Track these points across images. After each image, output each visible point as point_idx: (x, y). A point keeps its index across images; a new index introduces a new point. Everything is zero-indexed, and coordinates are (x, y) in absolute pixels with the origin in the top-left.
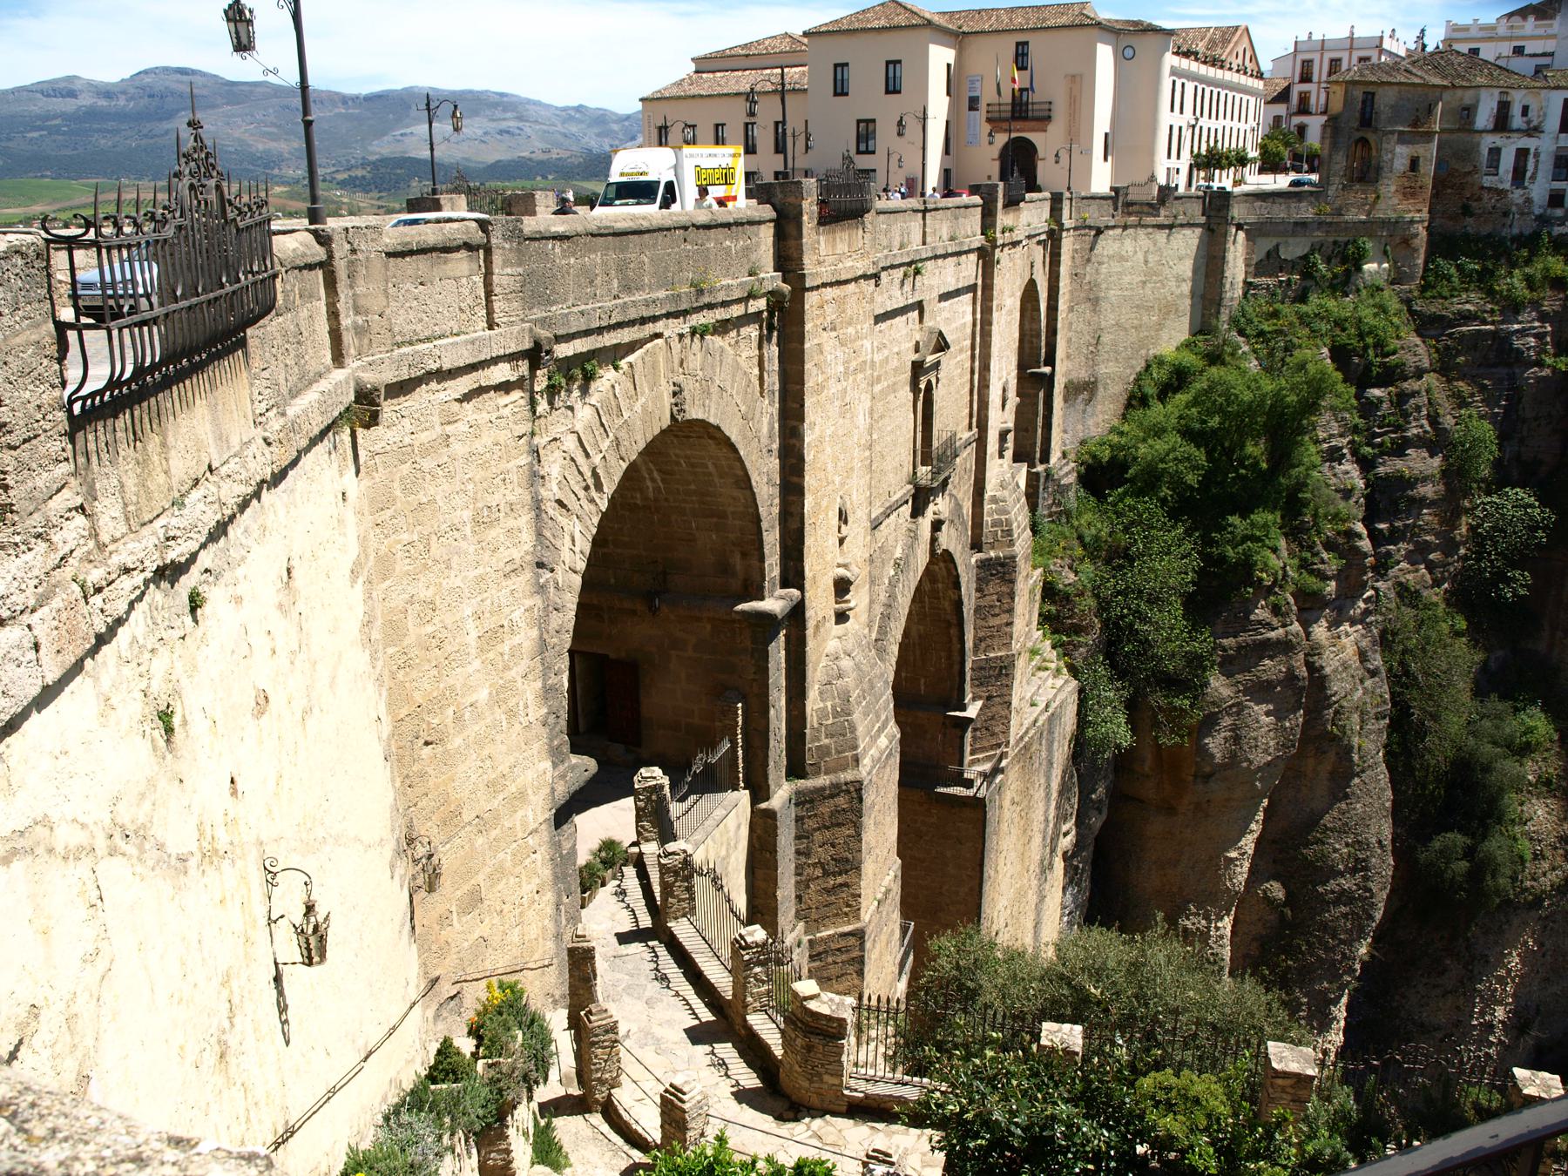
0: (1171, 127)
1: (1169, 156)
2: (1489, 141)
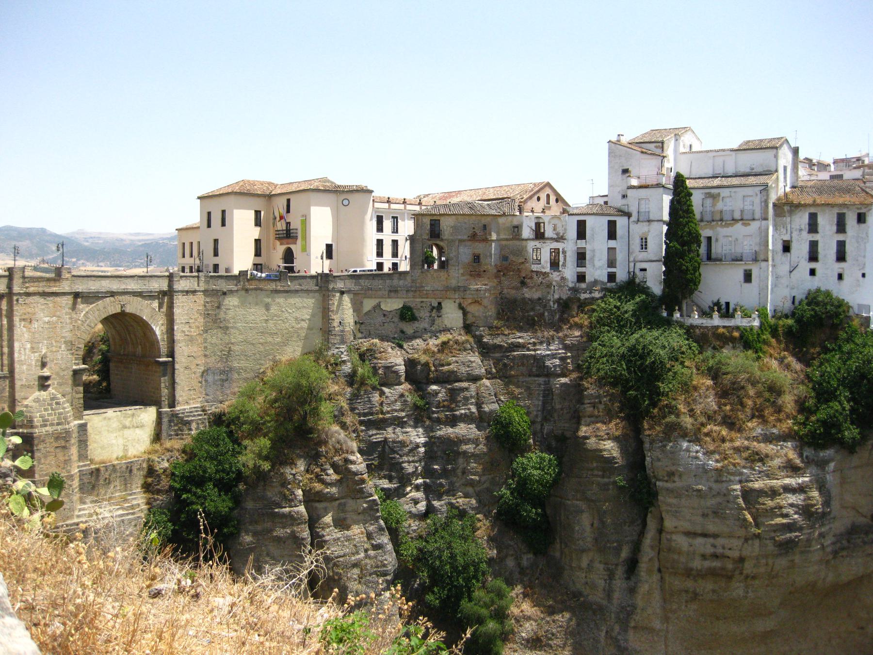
2: (531, 245)
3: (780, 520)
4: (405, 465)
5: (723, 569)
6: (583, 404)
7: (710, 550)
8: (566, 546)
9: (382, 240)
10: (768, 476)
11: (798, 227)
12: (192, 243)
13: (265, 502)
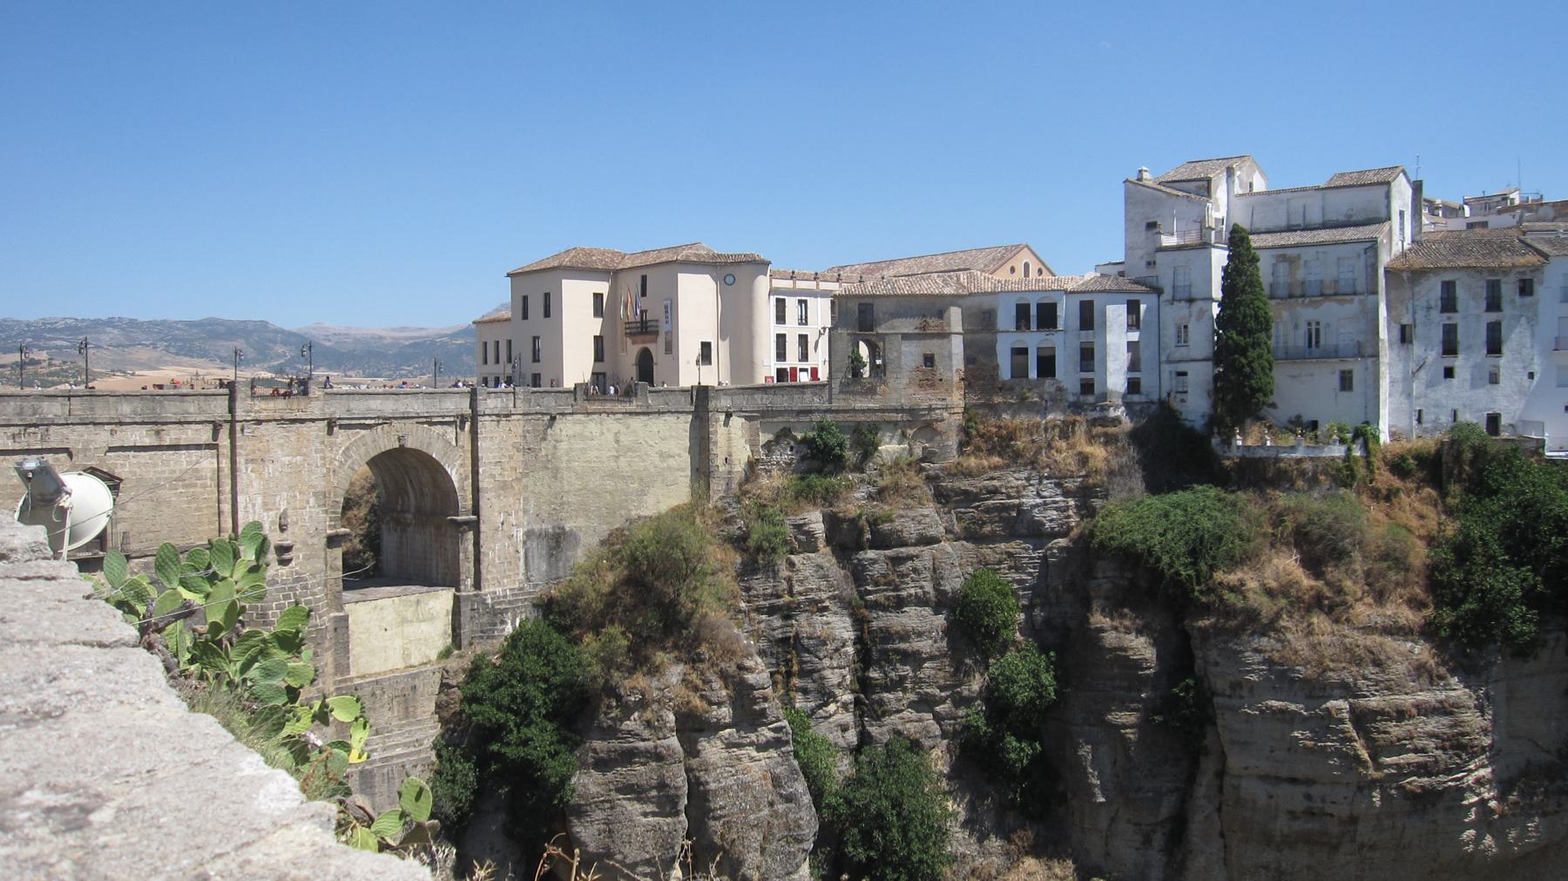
3: (1412, 757)
4: (827, 673)
7: (1300, 805)
9: (784, 336)
10: (1389, 689)
11: (1425, 304)
12: (498, 342)
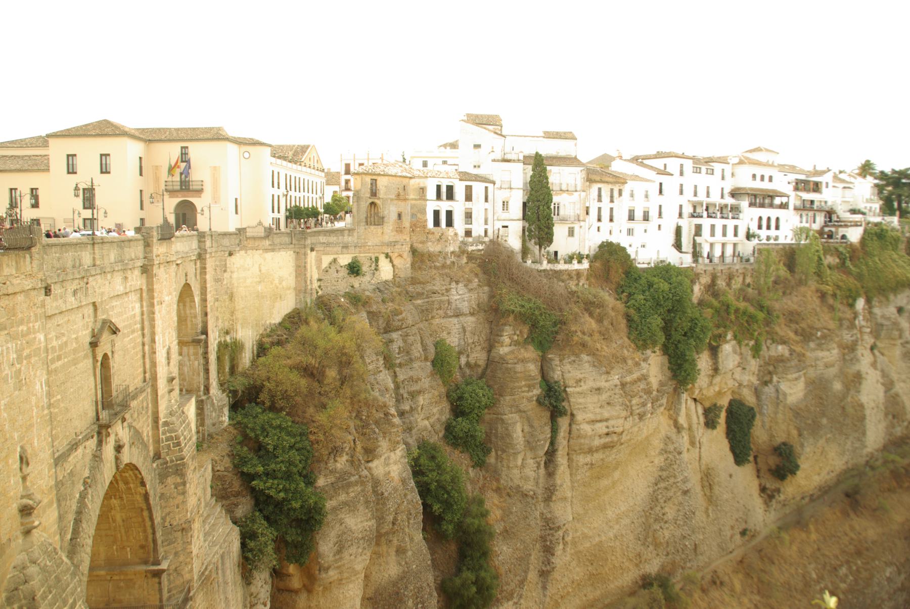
0: (273, 195)
1: (273, 212)
5: (612, 442)
6: (502, 336)
7: (605, 430)
8: (504, 451)
10: (630, 372)
13: (338, 475)
